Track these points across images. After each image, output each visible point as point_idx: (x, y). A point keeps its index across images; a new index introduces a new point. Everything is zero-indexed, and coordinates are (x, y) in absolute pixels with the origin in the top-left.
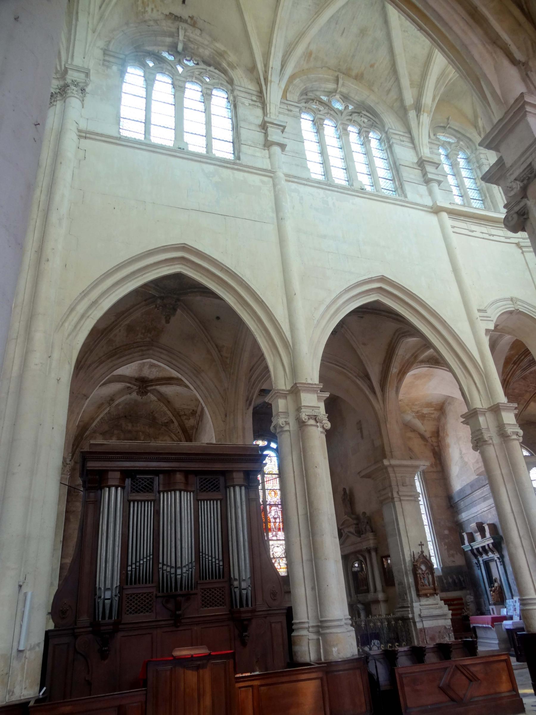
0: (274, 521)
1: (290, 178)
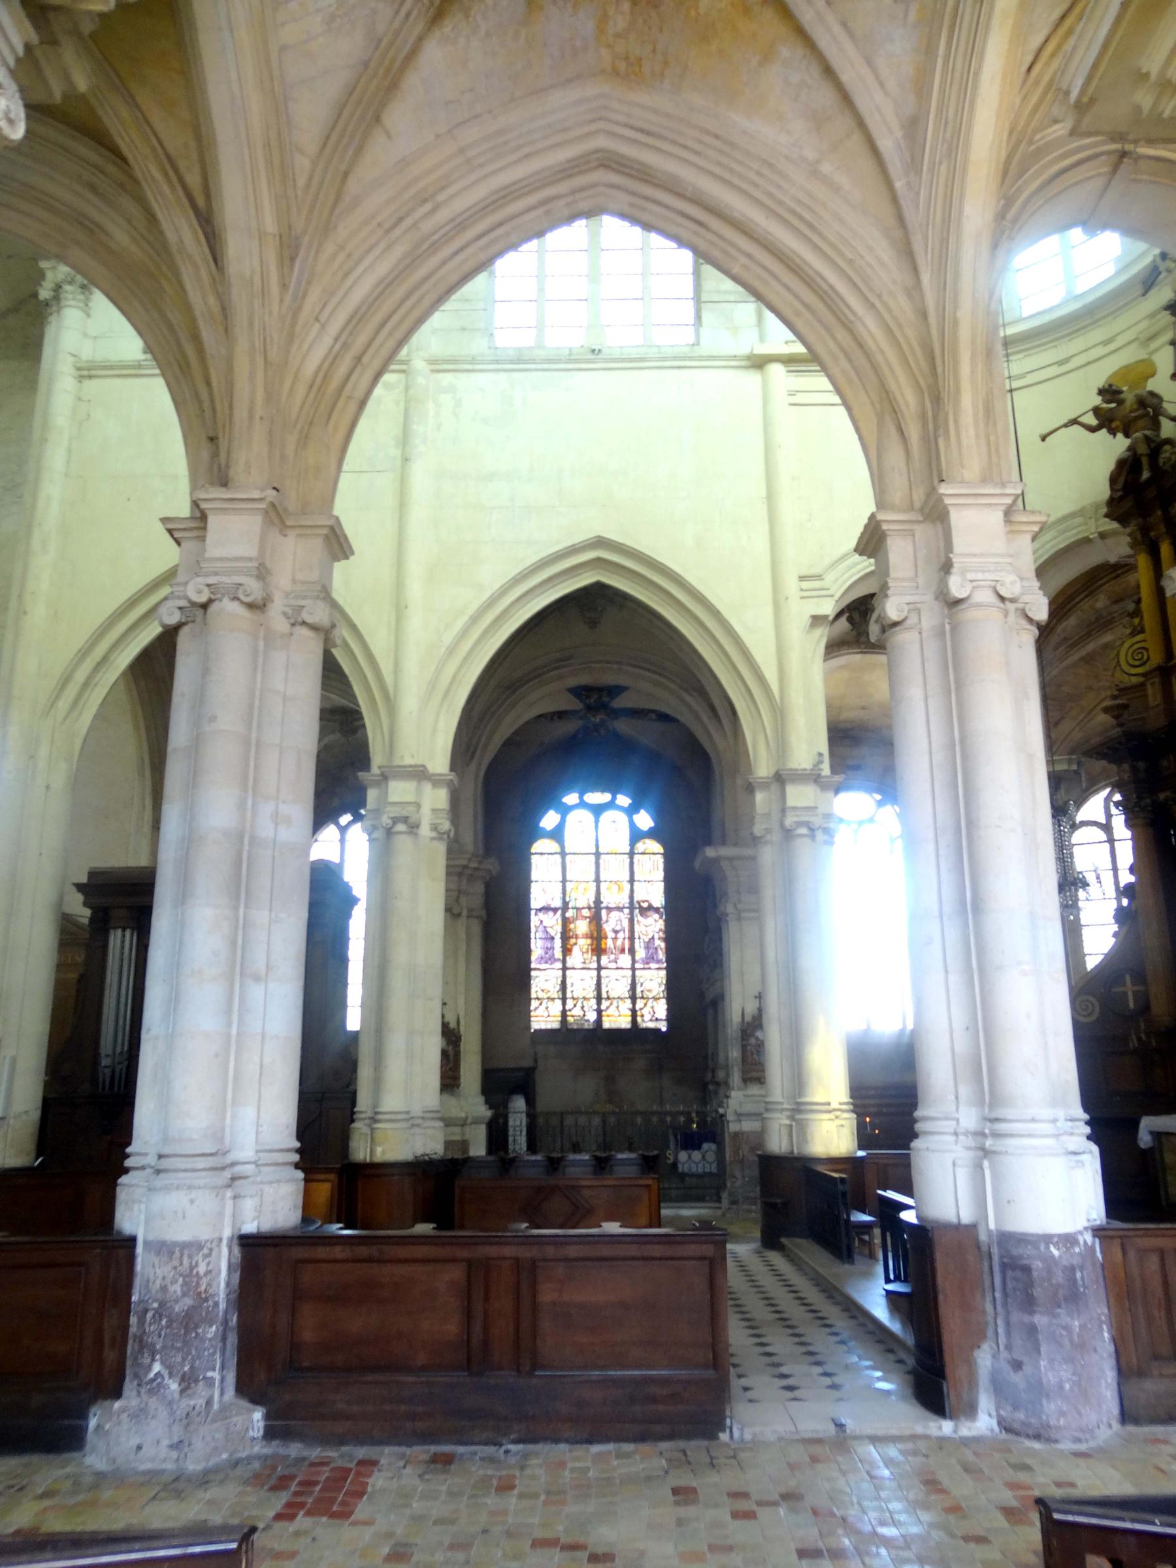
0: (613, 935)
1: (439, 365)
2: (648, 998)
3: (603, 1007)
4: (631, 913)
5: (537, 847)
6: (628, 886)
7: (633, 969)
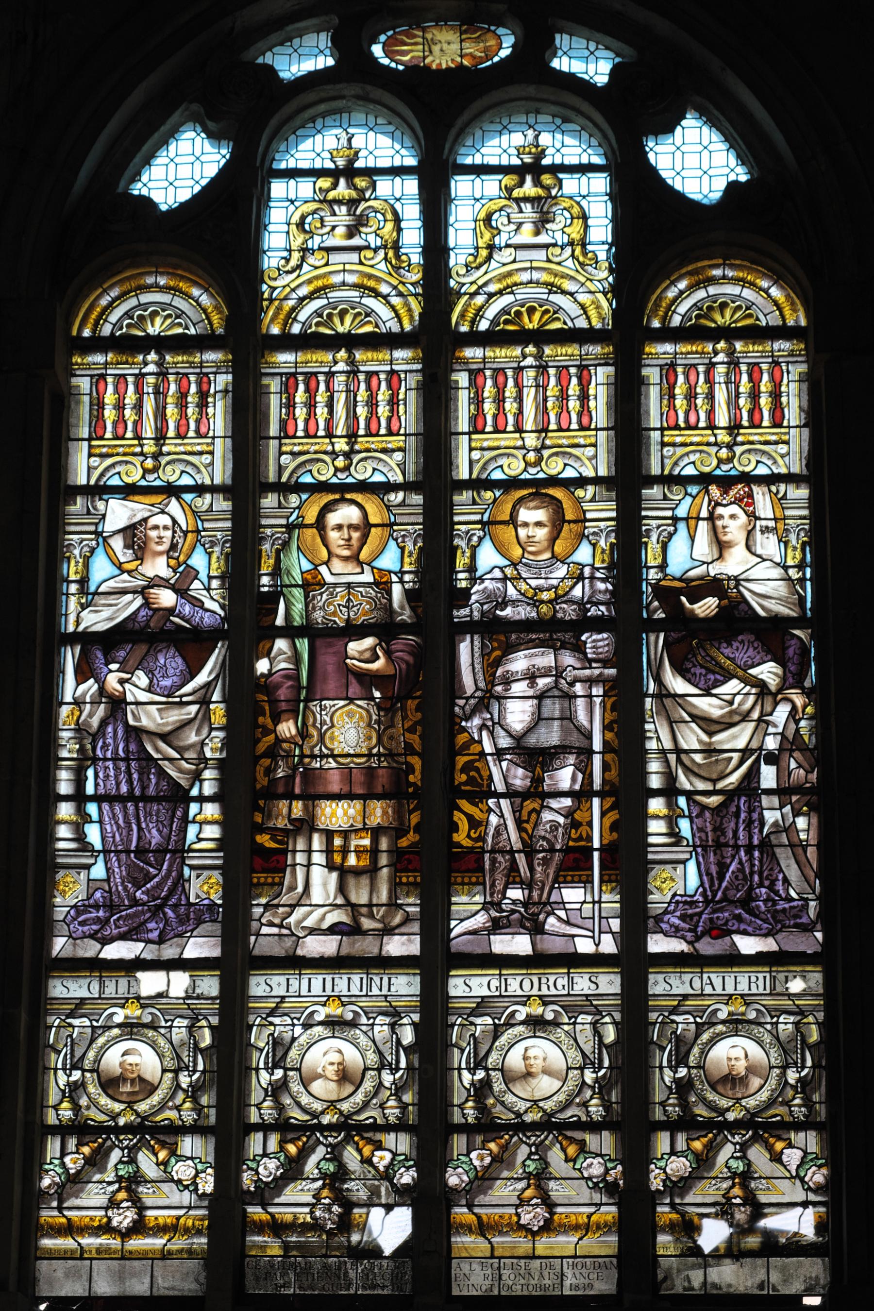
0: (520, 778)
2: (719, 1127)
4: (626, 657)
5: (114, 311)
6: (602, 511)
7: (633, 962)
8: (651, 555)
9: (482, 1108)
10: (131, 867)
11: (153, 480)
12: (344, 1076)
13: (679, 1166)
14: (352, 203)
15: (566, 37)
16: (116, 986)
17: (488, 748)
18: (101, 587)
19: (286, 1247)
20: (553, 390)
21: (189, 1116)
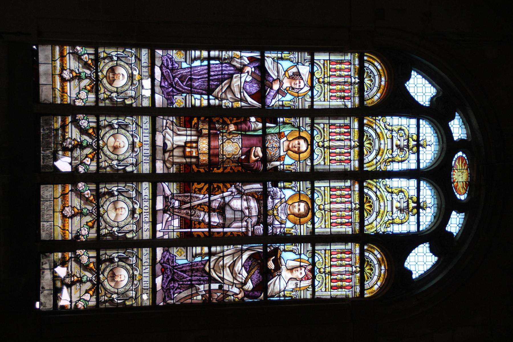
0: (215, 205)
2: (98, 272)
3: (81, 185)
4: (255, 239)
6: (303, 230)
7: (153, 243)
8: (288, 247)
9: (105, 194)
10: (186, 76)
11: (315, 81)
12: (115, 148)
13: (85, 260)
14: (408, 146)
15: (463, 217)
16: (146, 71)
17: (225, 194)
18: (281, 65)
19: (57, 130)
20: (344, 214)
21: (102, 96)
